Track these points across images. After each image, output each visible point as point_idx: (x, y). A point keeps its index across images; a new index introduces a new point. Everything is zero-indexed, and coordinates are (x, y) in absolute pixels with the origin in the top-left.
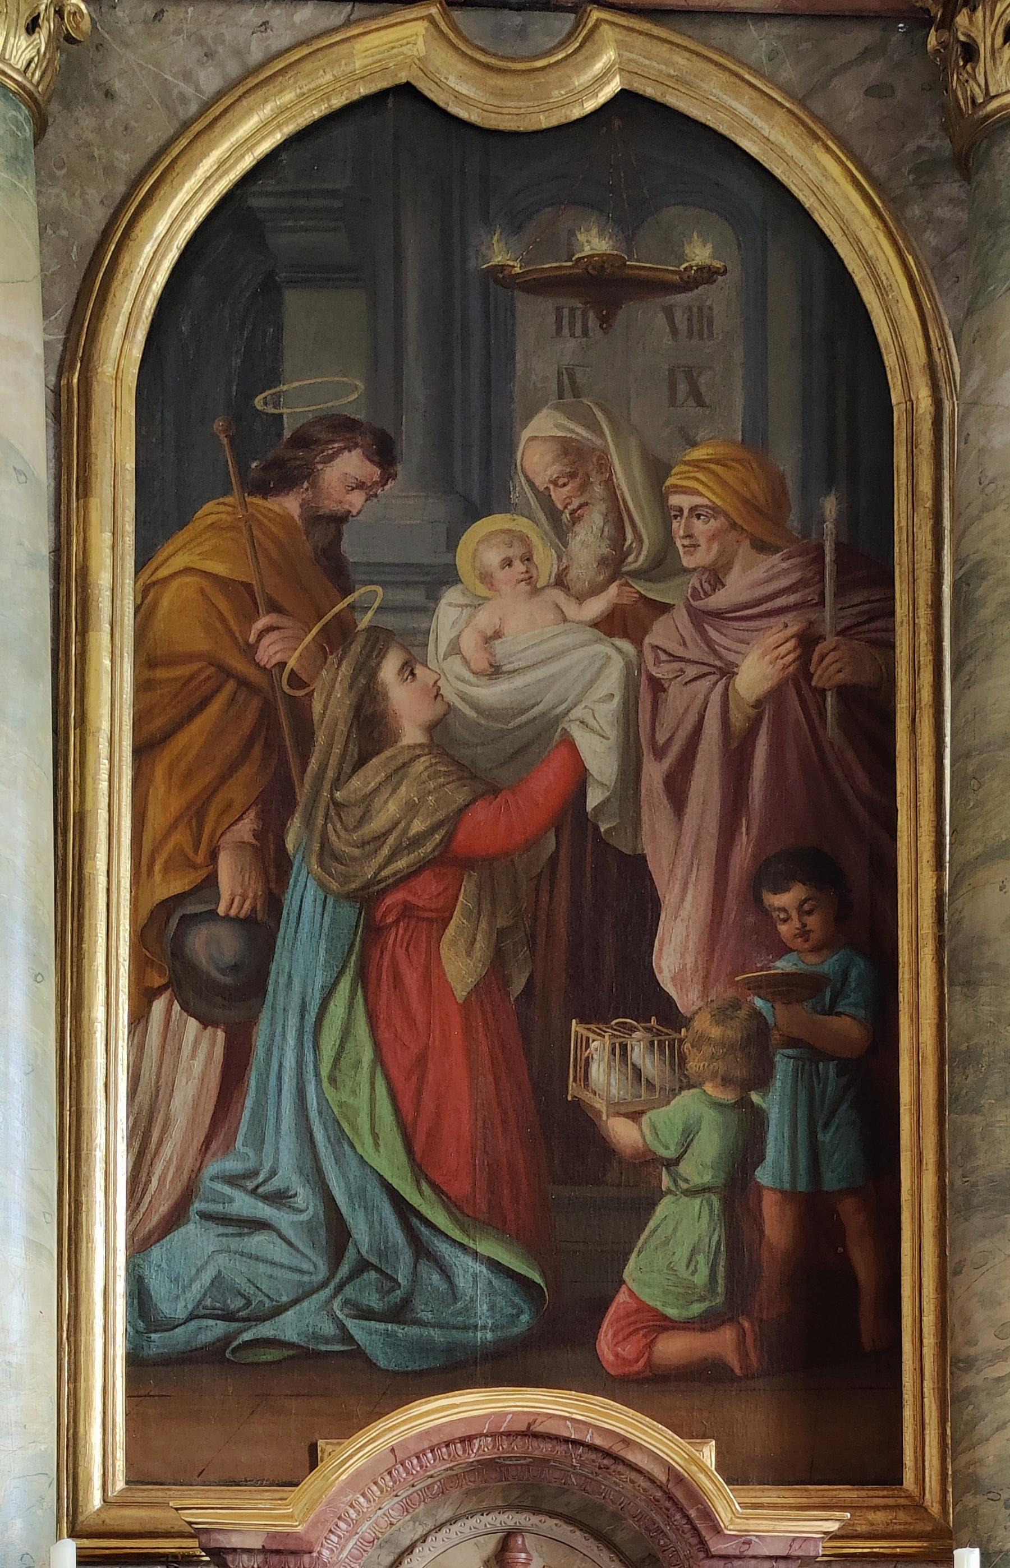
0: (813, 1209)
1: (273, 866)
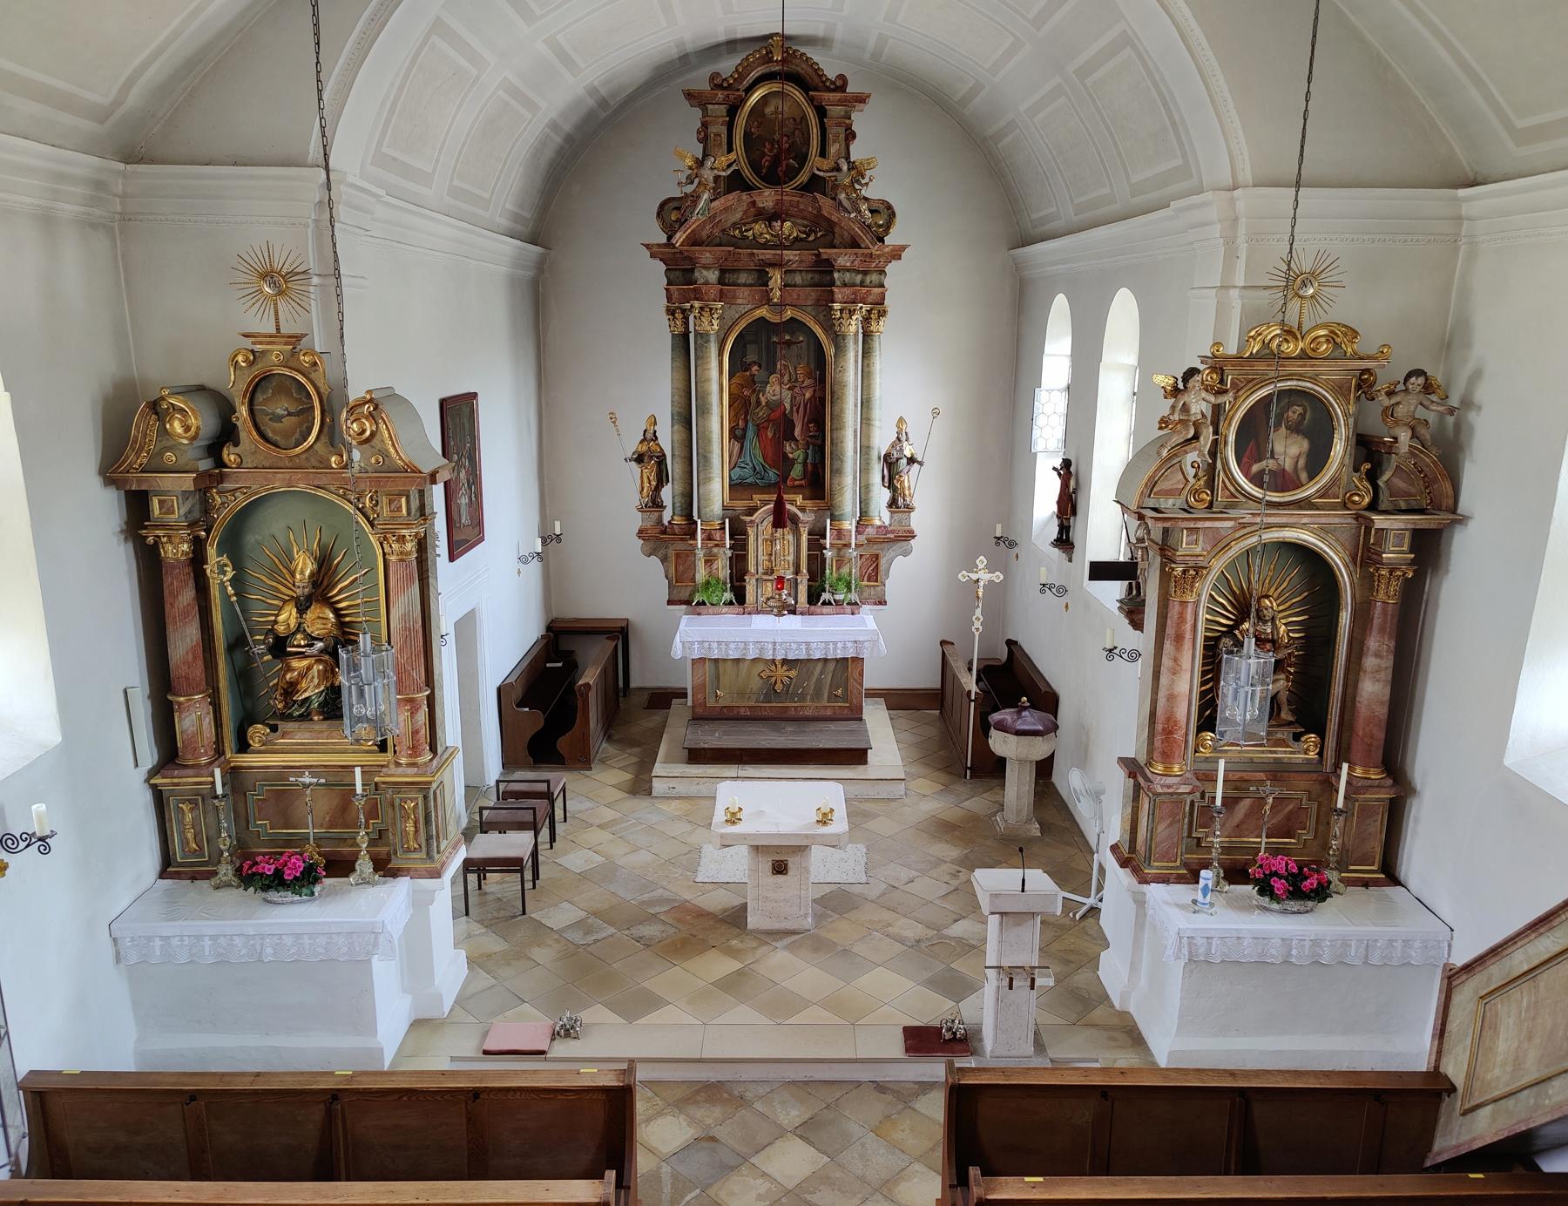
0: (814, 465)
1: (746, 422)
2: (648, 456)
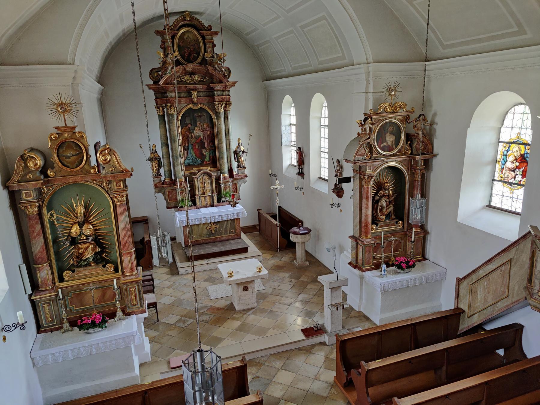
0: (213, 156)
1: (188, 144)
2: (154, 158)
